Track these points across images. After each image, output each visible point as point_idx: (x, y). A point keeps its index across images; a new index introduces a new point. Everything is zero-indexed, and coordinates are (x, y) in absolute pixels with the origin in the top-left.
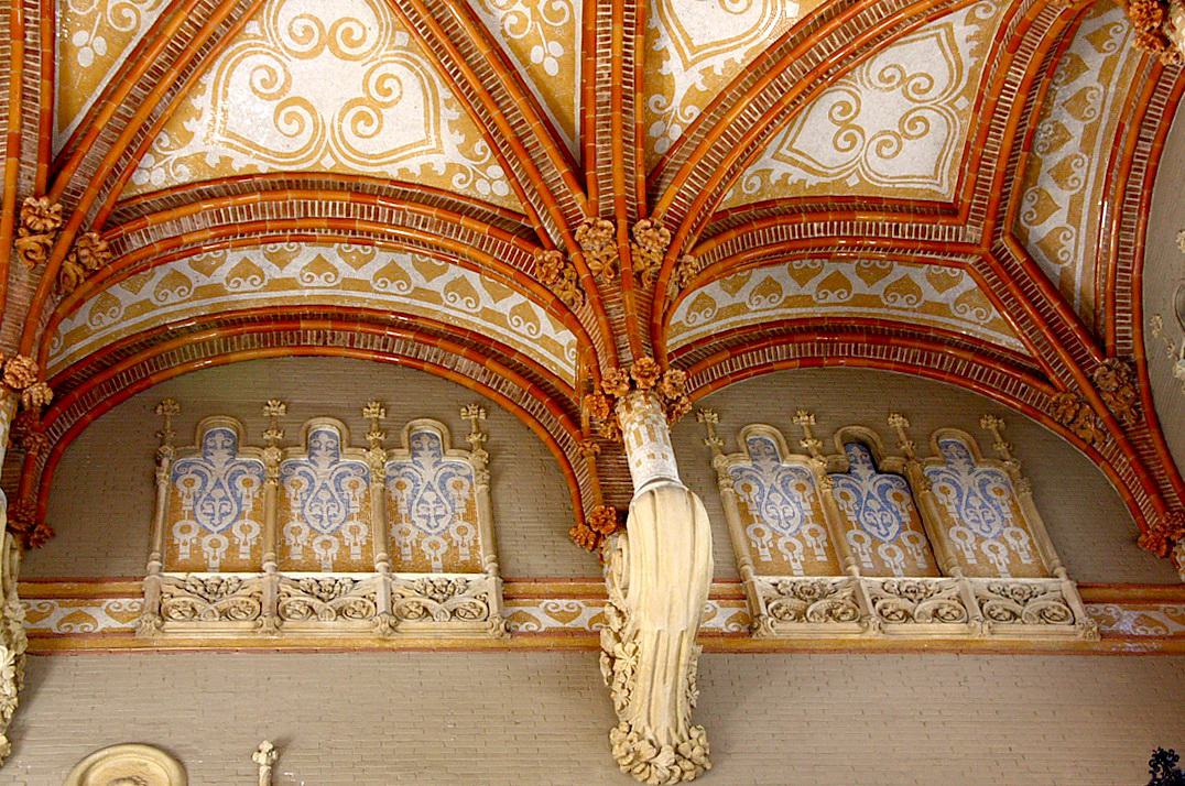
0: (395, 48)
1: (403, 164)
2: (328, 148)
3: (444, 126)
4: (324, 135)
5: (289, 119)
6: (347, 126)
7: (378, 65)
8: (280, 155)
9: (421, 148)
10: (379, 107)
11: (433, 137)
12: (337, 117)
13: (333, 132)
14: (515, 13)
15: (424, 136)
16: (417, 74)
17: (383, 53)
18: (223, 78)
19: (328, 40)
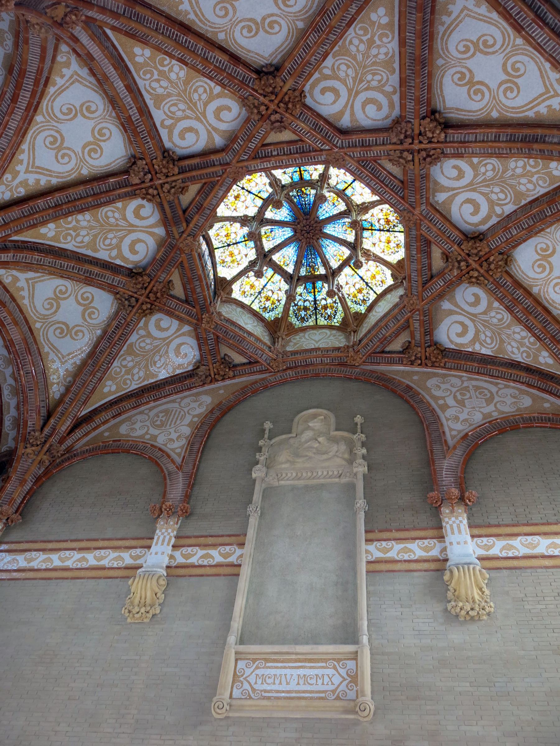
0: (445, 60)
1: (488, 14)
2: (514, 45)
3: (453, 16)
4: (510, 52)
5: (518, 70)
6: (497, 47)
7: (459, 59)
8: (536, 63)
9: (472, 14)
10: (476, 44)
11: (462, 16)
12: (497, 54)
13: (504, 50)
14: (382, 41)
15: (467, 18)
16: (446, 44)
17: (453, 62)
18: (525, 109)
19: (471, 83)
